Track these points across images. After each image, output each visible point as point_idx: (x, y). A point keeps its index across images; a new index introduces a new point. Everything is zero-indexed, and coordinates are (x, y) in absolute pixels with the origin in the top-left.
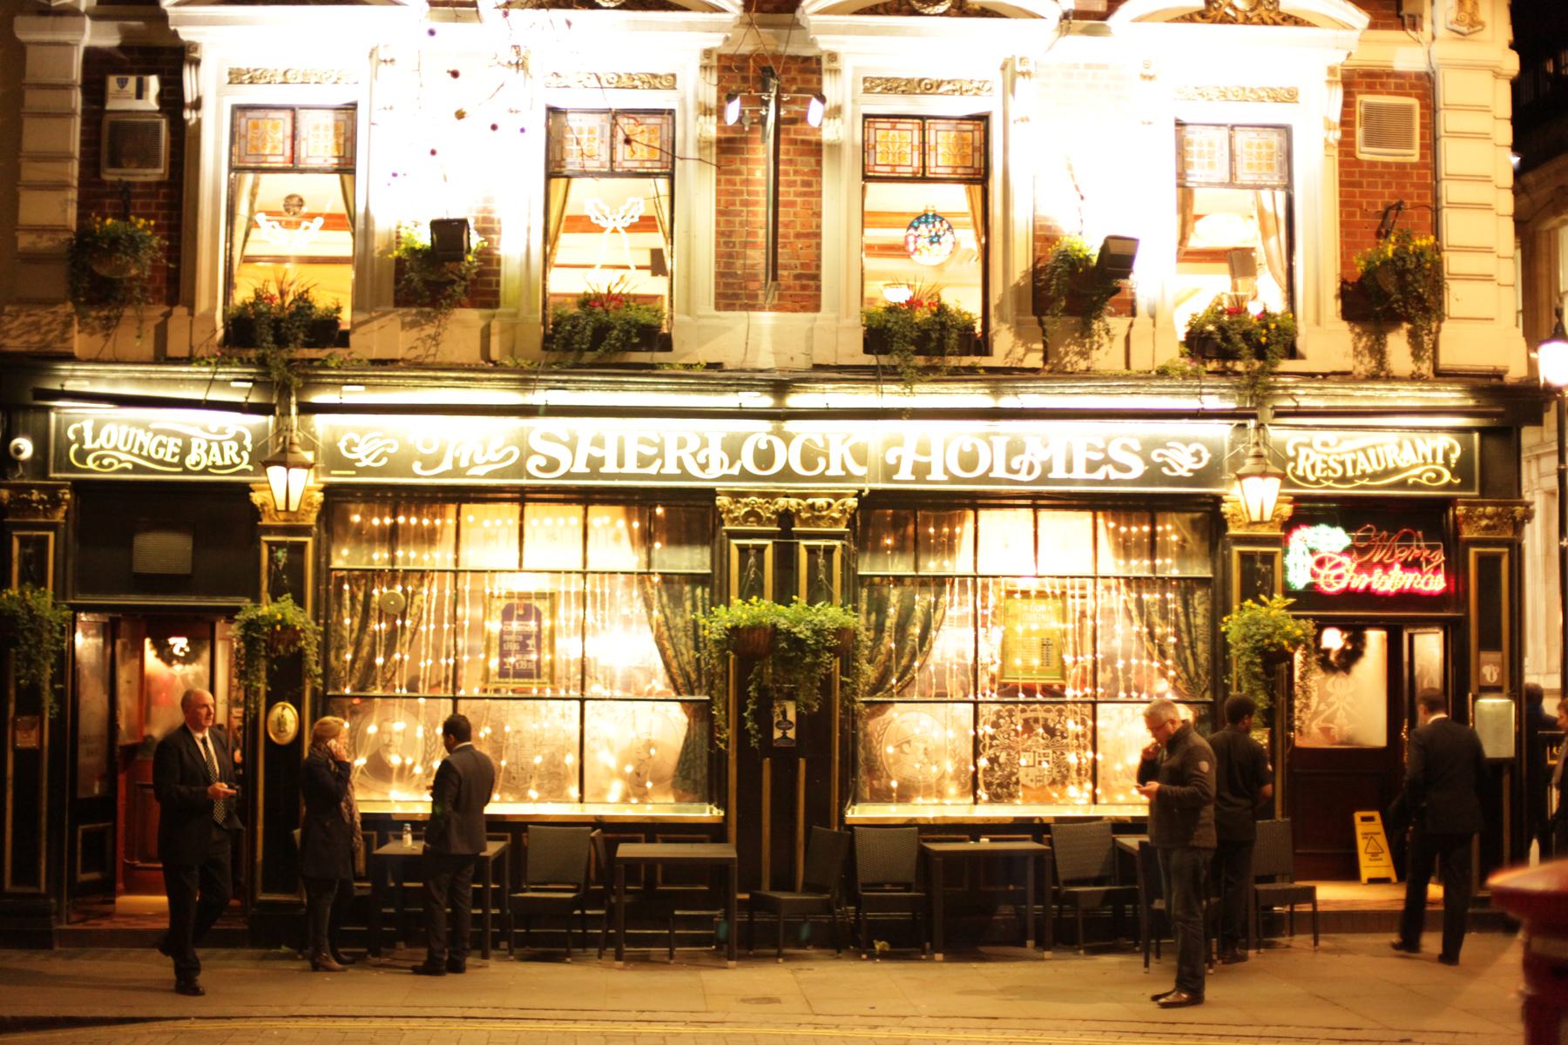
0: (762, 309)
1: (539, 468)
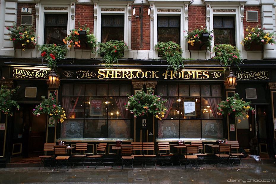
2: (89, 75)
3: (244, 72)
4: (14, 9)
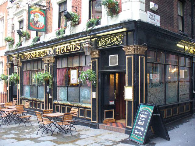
3: (104, 38)
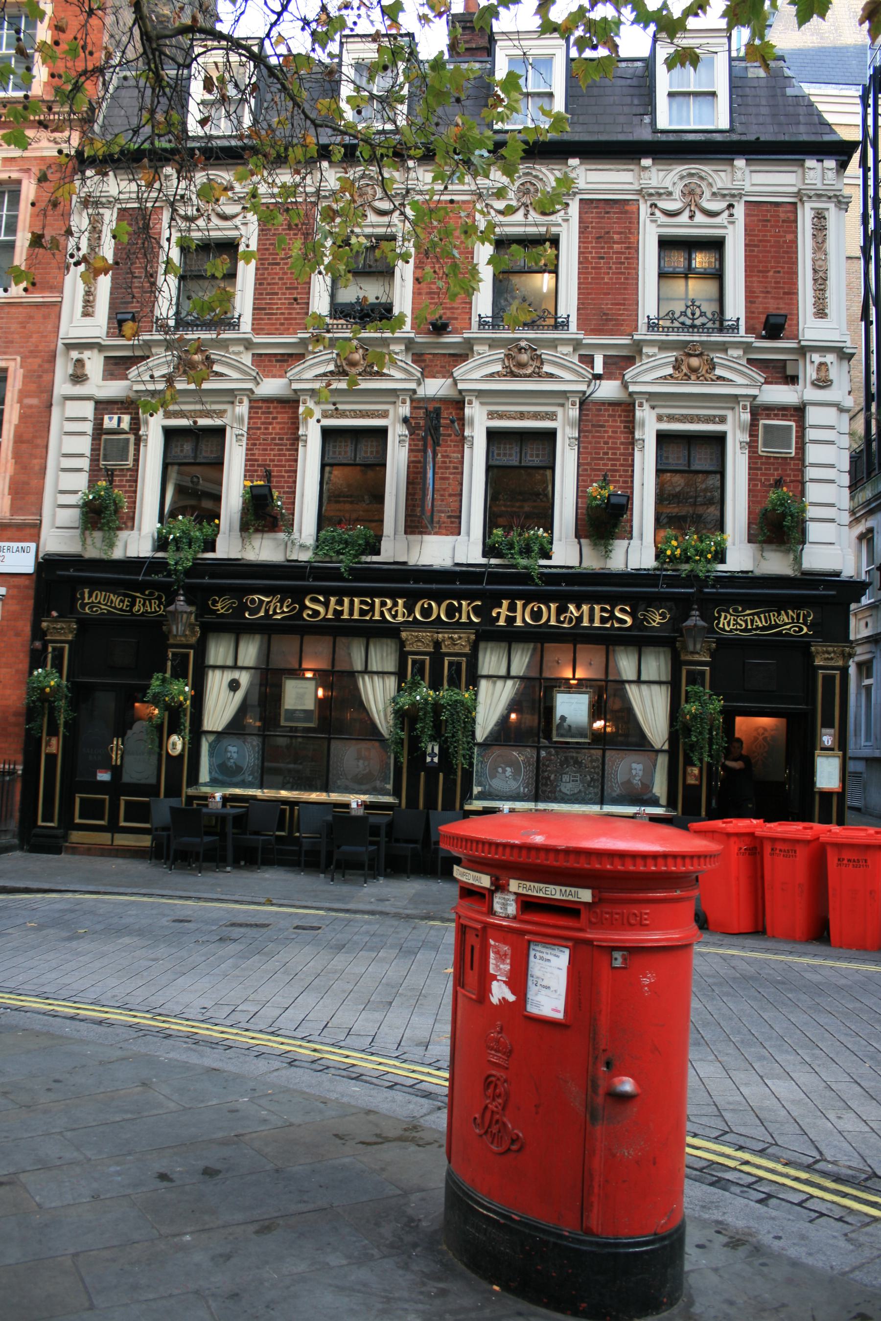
0: (429, 534)
1: (308, 615)
2: (281, 607)
4: (84, 419)
